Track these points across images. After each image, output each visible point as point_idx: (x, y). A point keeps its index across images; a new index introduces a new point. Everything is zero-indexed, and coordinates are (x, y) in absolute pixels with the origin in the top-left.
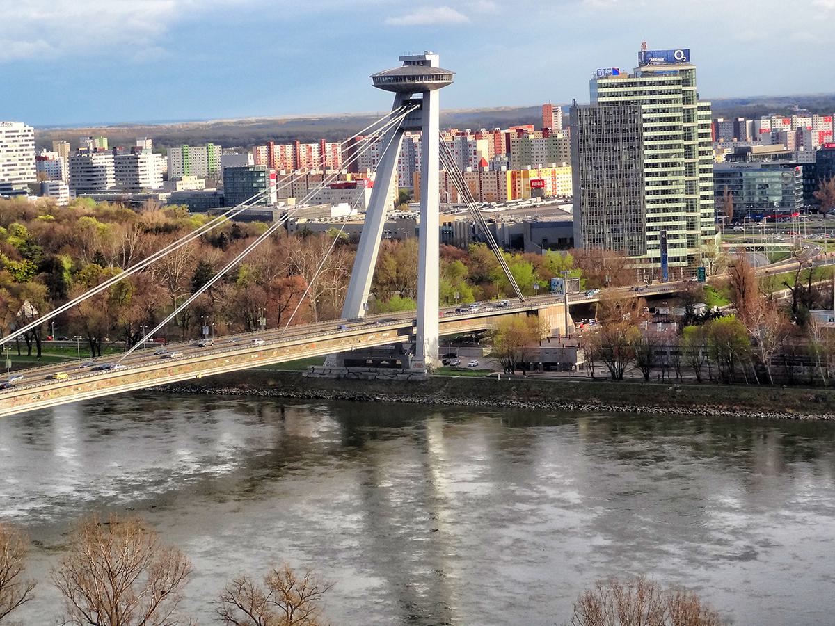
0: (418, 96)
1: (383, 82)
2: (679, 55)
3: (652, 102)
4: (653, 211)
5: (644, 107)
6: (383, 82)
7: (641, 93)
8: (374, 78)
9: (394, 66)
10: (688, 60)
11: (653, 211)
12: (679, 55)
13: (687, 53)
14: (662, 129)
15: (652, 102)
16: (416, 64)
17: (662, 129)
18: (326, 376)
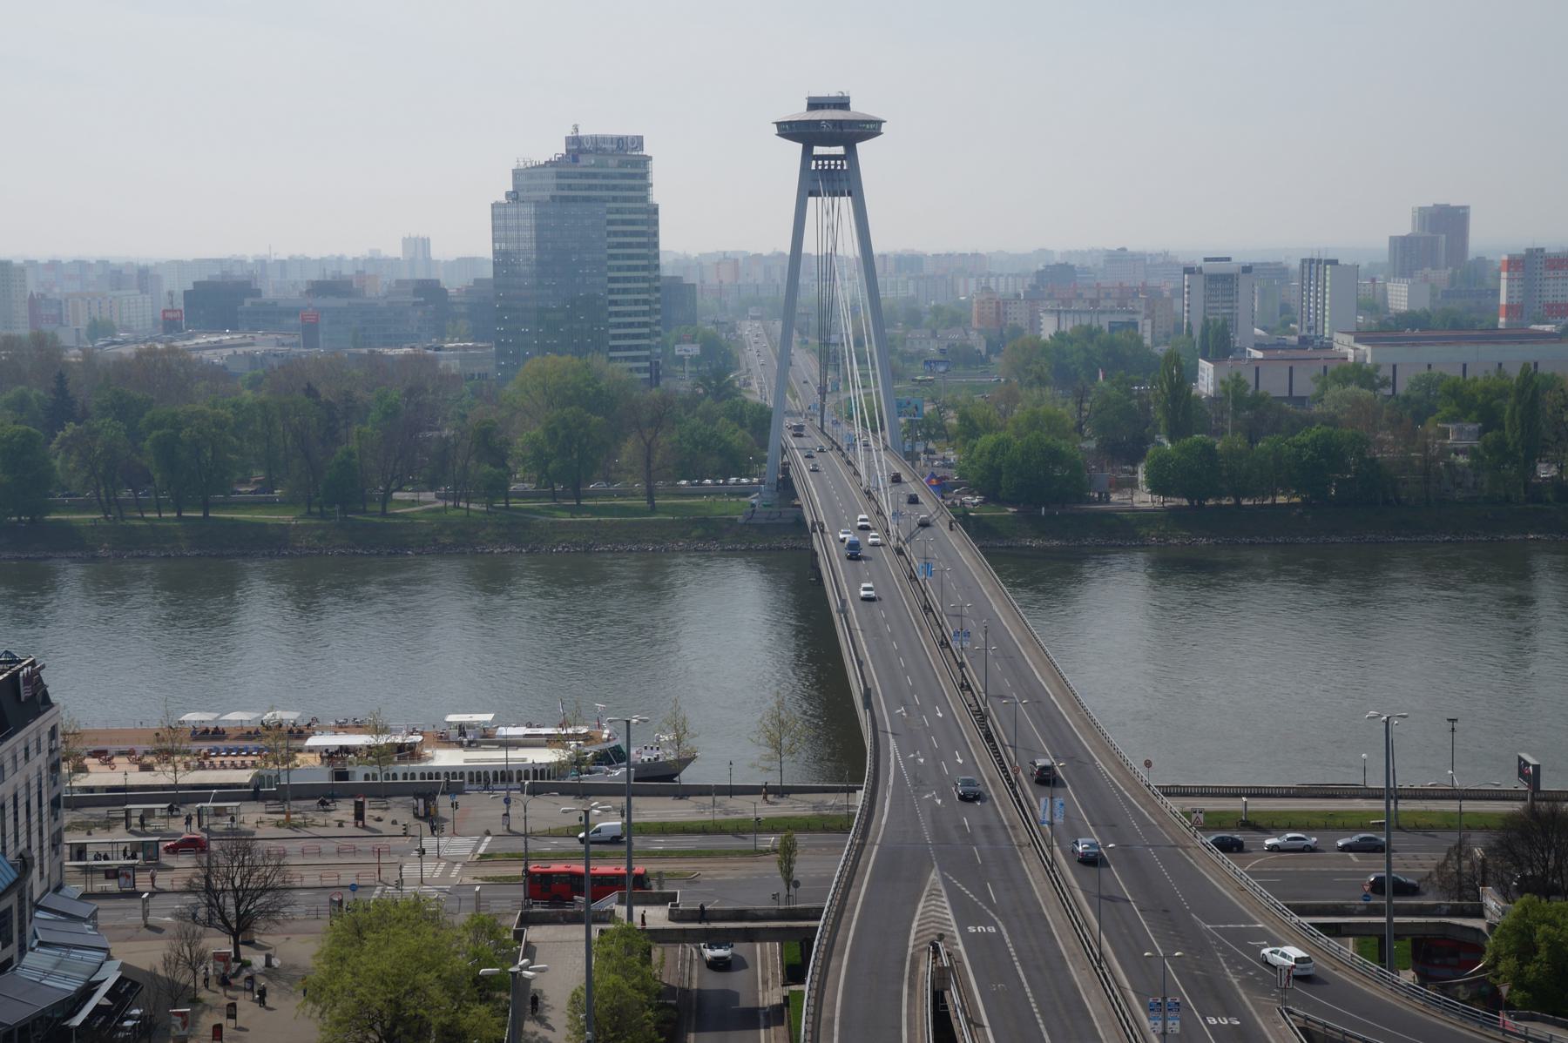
0: (840, 150)
1: (789, 130)
2: (633, 144)
3: (615, 199)
4: (615, 337)
5: (608, 205)
6: (789, 130)
7: (601, 187)
8: (779, 124)
9: (797, 111)
11: (615, 337)
13: (638, 142)
14: (625, 234)
15: (615, 199)
17: (625, 234)
18: (778, 521)
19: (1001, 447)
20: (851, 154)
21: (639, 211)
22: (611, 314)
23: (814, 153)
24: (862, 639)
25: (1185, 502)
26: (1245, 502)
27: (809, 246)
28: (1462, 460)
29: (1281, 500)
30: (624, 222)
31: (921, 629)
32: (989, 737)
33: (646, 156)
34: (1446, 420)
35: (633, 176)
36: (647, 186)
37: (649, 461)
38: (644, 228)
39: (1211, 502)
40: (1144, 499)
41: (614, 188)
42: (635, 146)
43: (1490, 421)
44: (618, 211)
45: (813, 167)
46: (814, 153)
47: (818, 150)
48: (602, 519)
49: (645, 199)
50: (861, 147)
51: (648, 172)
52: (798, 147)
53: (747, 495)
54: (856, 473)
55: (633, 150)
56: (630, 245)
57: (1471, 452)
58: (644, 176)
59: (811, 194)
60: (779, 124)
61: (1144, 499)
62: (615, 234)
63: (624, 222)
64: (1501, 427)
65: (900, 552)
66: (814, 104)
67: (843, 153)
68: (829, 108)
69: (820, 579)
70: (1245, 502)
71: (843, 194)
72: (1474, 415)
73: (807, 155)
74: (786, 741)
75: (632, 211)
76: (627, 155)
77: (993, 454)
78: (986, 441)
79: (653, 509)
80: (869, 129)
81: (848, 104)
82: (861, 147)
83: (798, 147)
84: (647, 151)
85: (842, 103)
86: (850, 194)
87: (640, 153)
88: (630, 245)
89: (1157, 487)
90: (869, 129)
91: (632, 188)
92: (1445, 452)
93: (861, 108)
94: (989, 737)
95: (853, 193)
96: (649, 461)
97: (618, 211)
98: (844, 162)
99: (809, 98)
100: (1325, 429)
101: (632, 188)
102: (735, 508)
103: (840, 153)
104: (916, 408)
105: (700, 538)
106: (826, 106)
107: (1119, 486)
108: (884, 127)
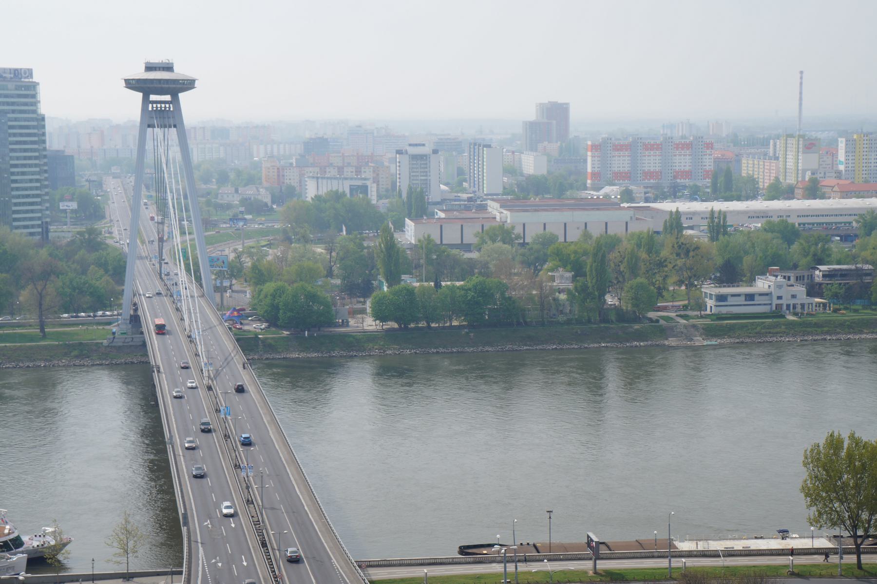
0: (168, 98)
1: (132, 84)
2: (25, 74)
3: (13, 112)
4: (16, 204)
5: (9, 115)
6: (132, 84)
8: (126, 80)
9: (139, 73)
10: (32, 78)
11: (16, 204)
12: (25, 74)
13: (29, 73)
14: (21, 135)
15: (13, 112)
16: (162, 69)
17: (21, 135)
18: (130, 344)
19: (278, 292)
20: (175, 100)
21: (32, 119)
22: (13, 189)
23: (151, 99)
24: (183, 463)
25: (396, 326)
26: (433, 325)
27: (149, 158)
28: (563, 297)
29: (455, 323)
30: (21, 127)
31: (222, 453)
32: (264, 545)
33: (35, 82)
34: (552, 270)
35: (26, 96)
36: (35, 104)
37: (41, 305)
38: (35, 131)
39: (412, 325)
40: (370, 324)
41: (13, 104)
42: (27, 75)
43: (578, 271)
44: (16, 120)
45: (150, 109)
46: (151, 99)
47: (153, 97)
48: (7, 345)
49: (34, 112)
50: (182, 96)
51: (37, 93)
52: (140, 95)
53: (109, 324)
54: (182, 319)
55: (25, 78)
56: (25, 143)
57: (568, 292)
58: (34, 96)
59: (149, 126)
60: (126, 80)
61: (370, 324)
62: (15, 135)
63: (21, 127)
64: (585, 275)
65: (210, 388)
66: (150, 68)
67: (170, 100)
68: (159, 70)
69: (157, 405)
70: (433, 325)
71: (170, 127)
72: (569, 267)
73: (146, 100)
74: (131, 544)
75: (26, 120)
76: (22, 82)
77: (274, 296)
78: (269, 287)
79: (44, 336)
80: (188, 84)
81: (172, 68)
82: (180, 95)
83: (140, 95)
84: (35, 79)
85: (169, 68)
86: (175, 126)
87: (31, 80)
88: (25, 143)
89: (379, 316)
90: (188, 84)
91: (26, 104)
92: (553, 290)
93: (181, 71)
94: (264, 545)
95: (178, 126)
96: (41, 305)
97: (16, 120)
98: (171, 105)
99: (146, 63)
100: (481, 279)
101: (26, 104)
102: (99, 335)
103: (168, 100)
104: (223, 262)
105: (77, 357)
106: (157, 69)
107: (353, 313)
108: (197, 84)
